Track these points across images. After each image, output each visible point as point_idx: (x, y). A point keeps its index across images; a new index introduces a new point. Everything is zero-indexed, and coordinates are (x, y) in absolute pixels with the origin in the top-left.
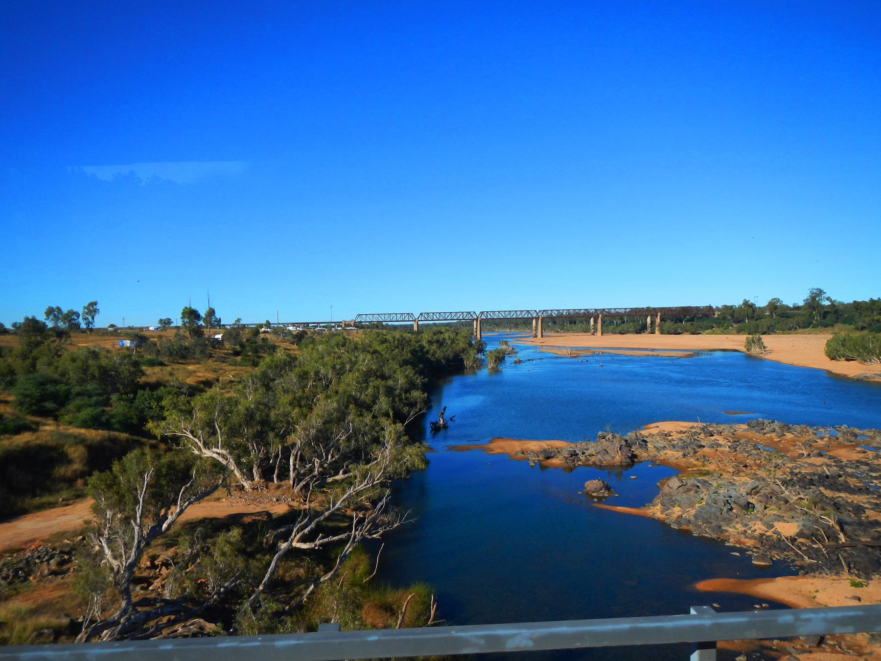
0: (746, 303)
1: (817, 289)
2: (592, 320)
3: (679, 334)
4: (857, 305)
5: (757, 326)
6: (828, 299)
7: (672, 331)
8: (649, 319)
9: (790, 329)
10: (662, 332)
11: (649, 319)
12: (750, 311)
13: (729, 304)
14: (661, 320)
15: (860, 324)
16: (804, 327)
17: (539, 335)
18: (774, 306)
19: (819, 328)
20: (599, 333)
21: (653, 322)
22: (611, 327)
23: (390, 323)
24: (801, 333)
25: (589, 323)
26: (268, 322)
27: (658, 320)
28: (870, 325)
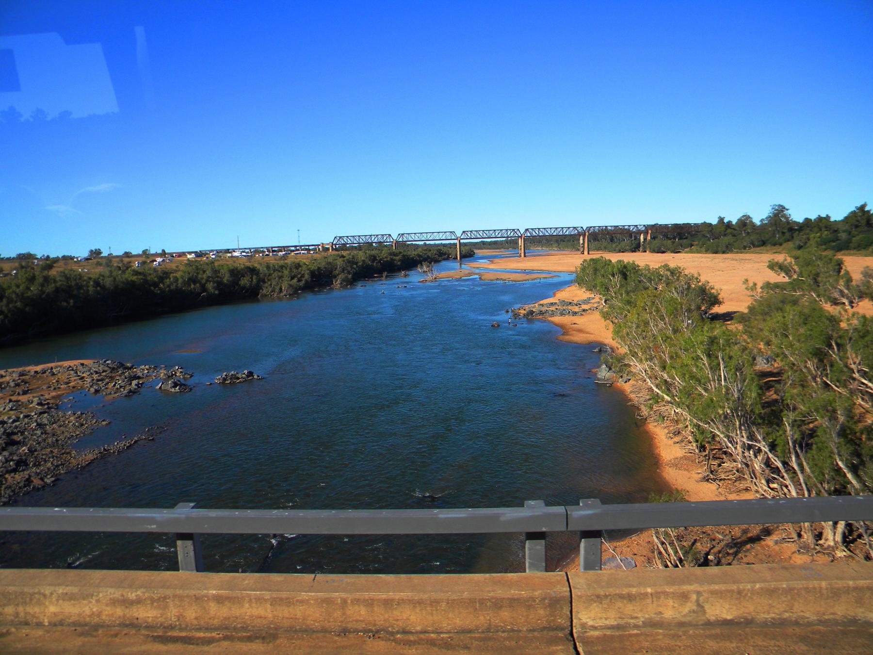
0: (721, 220)
1: (780, 206)
2: (581, 238)
3: (663, 252)
4: (807, 220)
5: (718, 246)
6: (785, 216)
7: (656, 250)
8: (642, 237)
9: (745, 248)
10: (650, 252)
11: (642, 237)
12: (723, 229)
13: (707, 222)
14: (654, 238)
15: (798, 243)
17: (523, 255)
18: (745, 222)
19: (768, 247)
20: (586, 252)
21: (645, 239)
22: (614, 246)
23: (428, 242)
24: (753, 253)
26: (163, 251)
27: (649, 238)
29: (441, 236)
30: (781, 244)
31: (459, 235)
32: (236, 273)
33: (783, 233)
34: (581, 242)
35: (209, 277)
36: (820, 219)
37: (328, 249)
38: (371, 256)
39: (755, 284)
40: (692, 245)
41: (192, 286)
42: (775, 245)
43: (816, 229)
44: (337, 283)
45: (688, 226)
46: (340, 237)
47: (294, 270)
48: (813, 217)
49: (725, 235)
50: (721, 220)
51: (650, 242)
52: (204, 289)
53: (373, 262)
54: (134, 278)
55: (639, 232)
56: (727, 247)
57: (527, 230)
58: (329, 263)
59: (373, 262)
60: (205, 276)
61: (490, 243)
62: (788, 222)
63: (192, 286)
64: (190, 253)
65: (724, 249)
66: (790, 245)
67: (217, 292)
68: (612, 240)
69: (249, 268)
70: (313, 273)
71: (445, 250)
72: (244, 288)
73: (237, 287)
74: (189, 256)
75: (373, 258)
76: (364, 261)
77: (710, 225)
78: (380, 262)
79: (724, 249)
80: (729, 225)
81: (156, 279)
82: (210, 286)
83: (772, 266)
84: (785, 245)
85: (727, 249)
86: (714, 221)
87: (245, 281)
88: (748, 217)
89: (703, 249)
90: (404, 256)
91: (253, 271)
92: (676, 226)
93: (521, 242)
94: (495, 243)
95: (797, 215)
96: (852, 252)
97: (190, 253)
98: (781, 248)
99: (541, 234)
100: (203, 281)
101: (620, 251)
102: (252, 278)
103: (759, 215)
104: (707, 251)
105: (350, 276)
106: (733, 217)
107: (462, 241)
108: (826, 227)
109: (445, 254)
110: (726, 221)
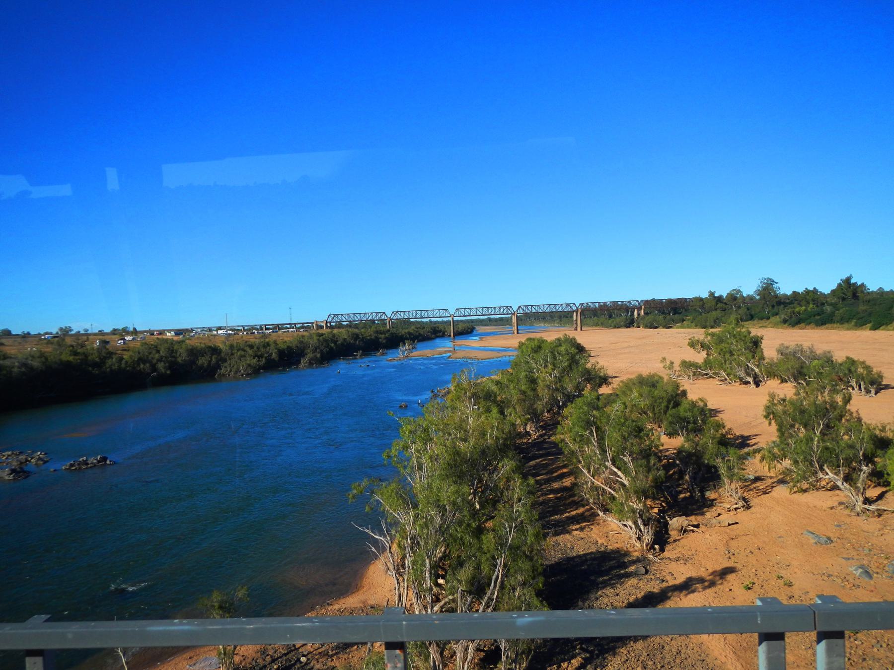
0: (712, 294)
3: (656, 328)
5: (706, 321)
11: (636, 312)
12: (714, 303)
14: (646, 314)
15: (783, 316)
16: (747, 320)
18: (734, 298)
20: (579, 329)
21: (639, 314)
23: (433, 320)
25: (572, 317)
26: (135, 329)
27: (642, 313)
28: (791, 317)
29: (430, 314)
30: (768, 318)
31: (452, 313)
32: (194, 353)
33: (773, 306)
34: (575, 318)
35: (162, 357)
36: (807, 292)
37: (322, 327)
38: (353, 334)
39: (672, 363)
40: (683, 320)
41: (142, 366)
42: (762, 319)
43: (804, 303)
44: (304, 361)
45: (683, 300)
46: (335, 315)
47: (262, 350)
48: (800, 290)
49: (716, 310)
50: (712, 294)
51: (643, 318)
52: (154, 368)
53: (355, 339)
54: (71, 358)
55: (633, 309)
56: (715, 321)
57: (520, 307)
58: (301, 342)
59: (355, 339)
60: (157, 356)
61: (496, 320)
62: (776, 296)
63: (142, 366)
64: (169, 331)
65: (713, 324)
66: (777, 319)
67: (168, 372)
68: (610, 316)
69: (210, 347)
70: (281, 353)
71: (441, 327)
72: (201, 367)
73: (194, 367)
74: (168, 334)
75: (356, 337)
76: (345, 339)
77: (701, 300)
78: (362, 340)
79: (713, 324)
80: (719, 299)
81: (97, 360)
82: (161, 366)
83: (692, 345)
84: (773, 319)
86: (705, 295)
87: (202, 361)
88: (739, 291)
89: (693, 324)
90: (392, 334)
91: (215, 350)
92: (670, 301)
93: (514, 320)
94: (501, 319)
95: (785, 288)
96: (835, 325)
97: (169, 331)
98: (769, 321)
99: (534, 311)
100: (154, 361)
101: (615, 327)
102: (211, 358)
103: (750, 288)
104: (696, 326)
105: (319, 355)
106: (723, 291)
107: (455, 319)
108: (813, 300)
109: (440, 331)
110: (717, 295)
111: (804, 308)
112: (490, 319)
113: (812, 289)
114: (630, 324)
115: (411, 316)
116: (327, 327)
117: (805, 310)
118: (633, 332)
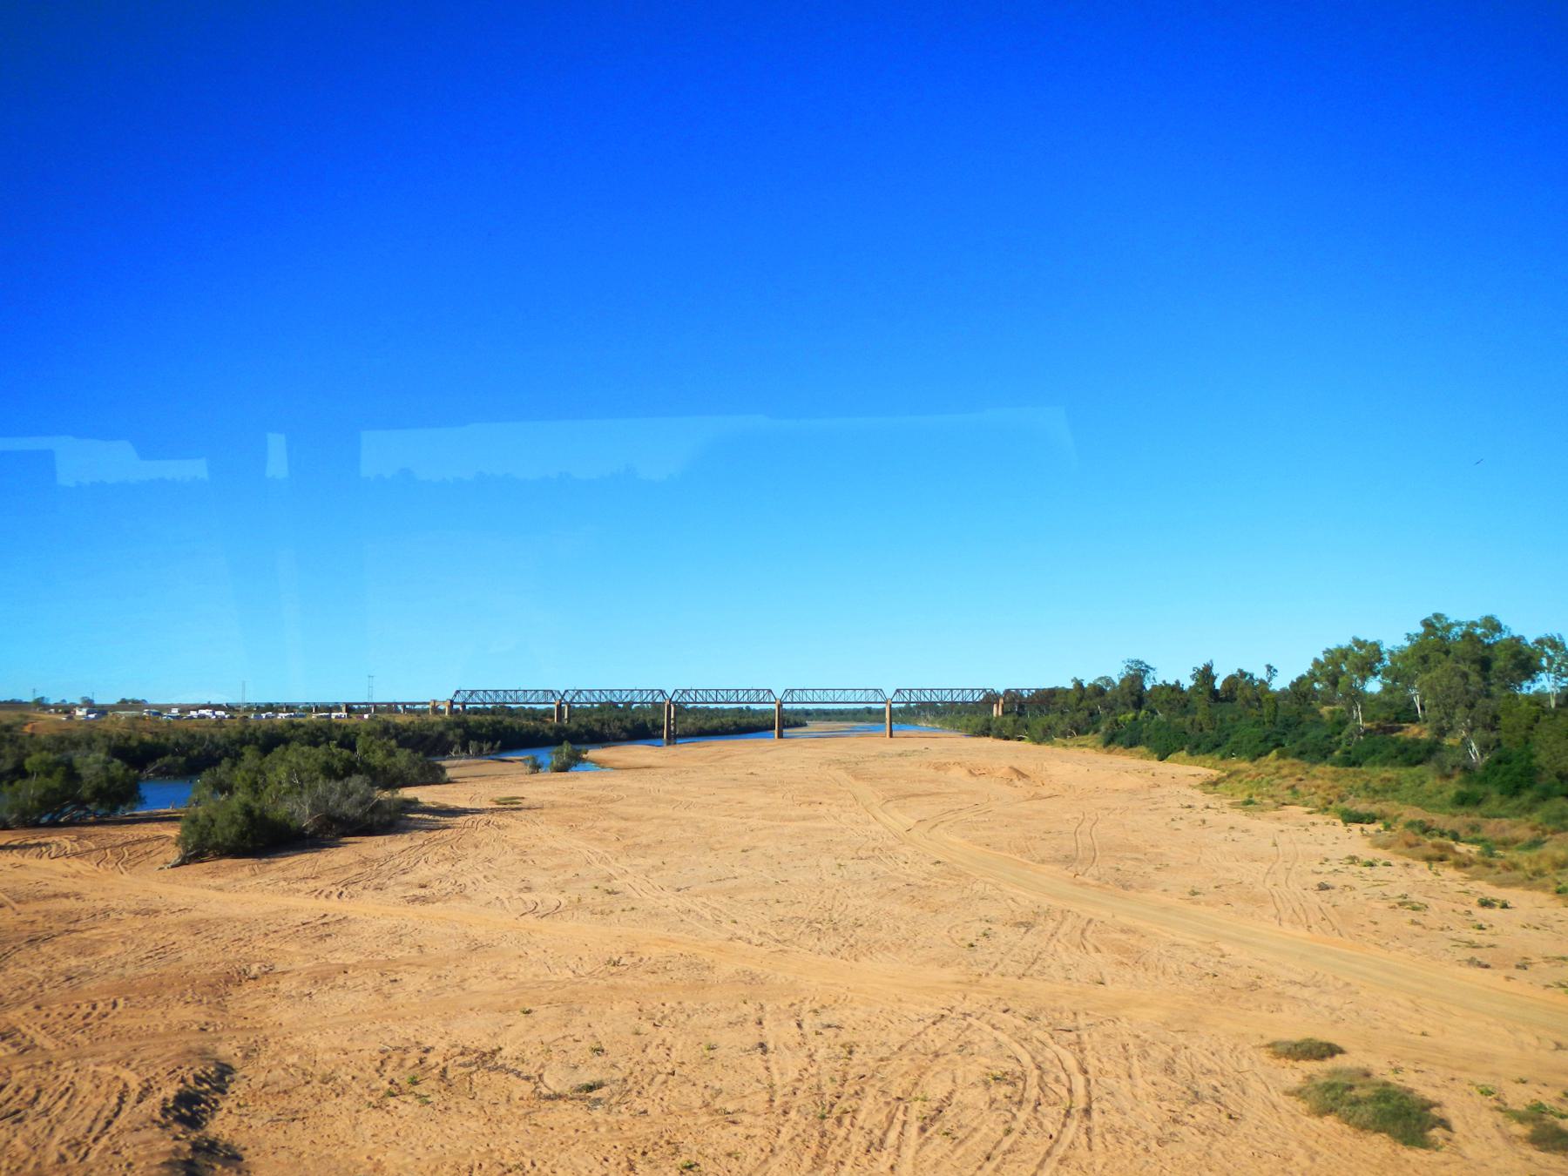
3: (1007, 738)
9: (1064, 735)
23: (753, 706)
36: (1165, 687)
46: (473, 692)
50: (1079, 684)
56: (1045, 731)
77: (1068, 691)
85: (1045, 736)
86: (1070, 686)
88: (1109, 681)
111: (1130, 715)
112: (869, 711)
113: (1172, 682)
114: (985, 732)
115: (699, 699)
116: (452, 712)
117: (1135, 719)
118: (988, 742)
